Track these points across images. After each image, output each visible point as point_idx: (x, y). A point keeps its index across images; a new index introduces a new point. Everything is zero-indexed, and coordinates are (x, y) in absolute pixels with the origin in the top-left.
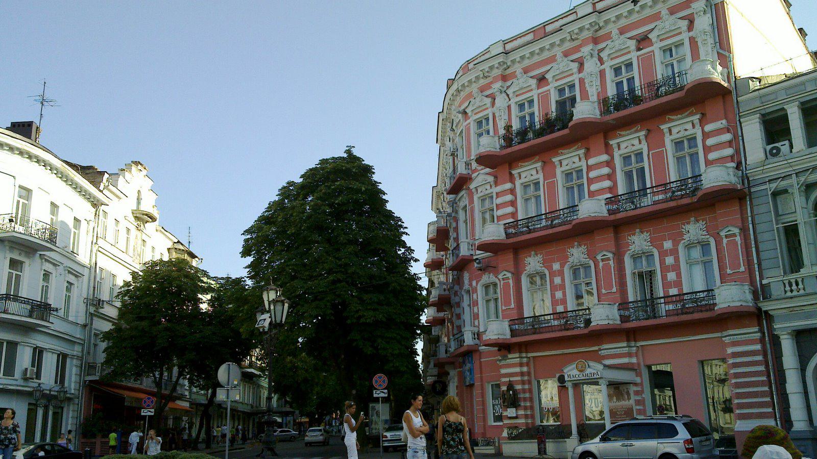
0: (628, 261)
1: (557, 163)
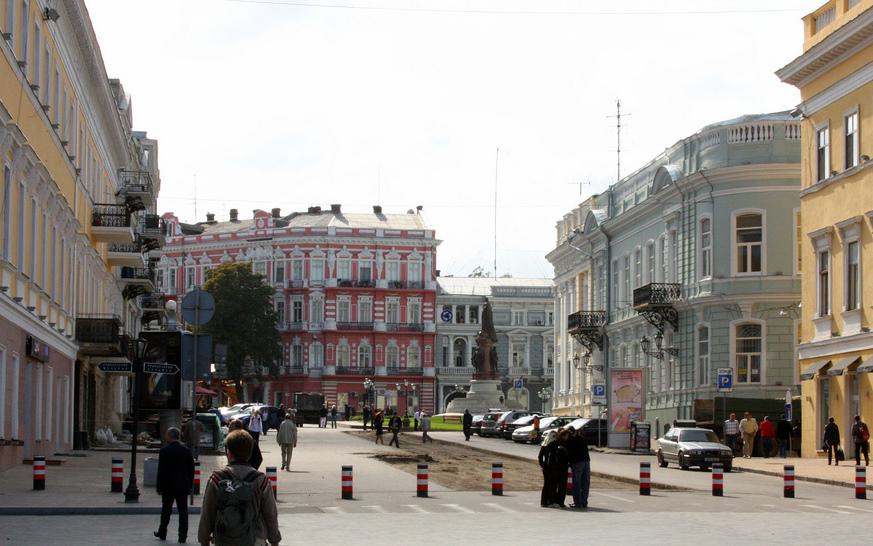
0: (386, 350)
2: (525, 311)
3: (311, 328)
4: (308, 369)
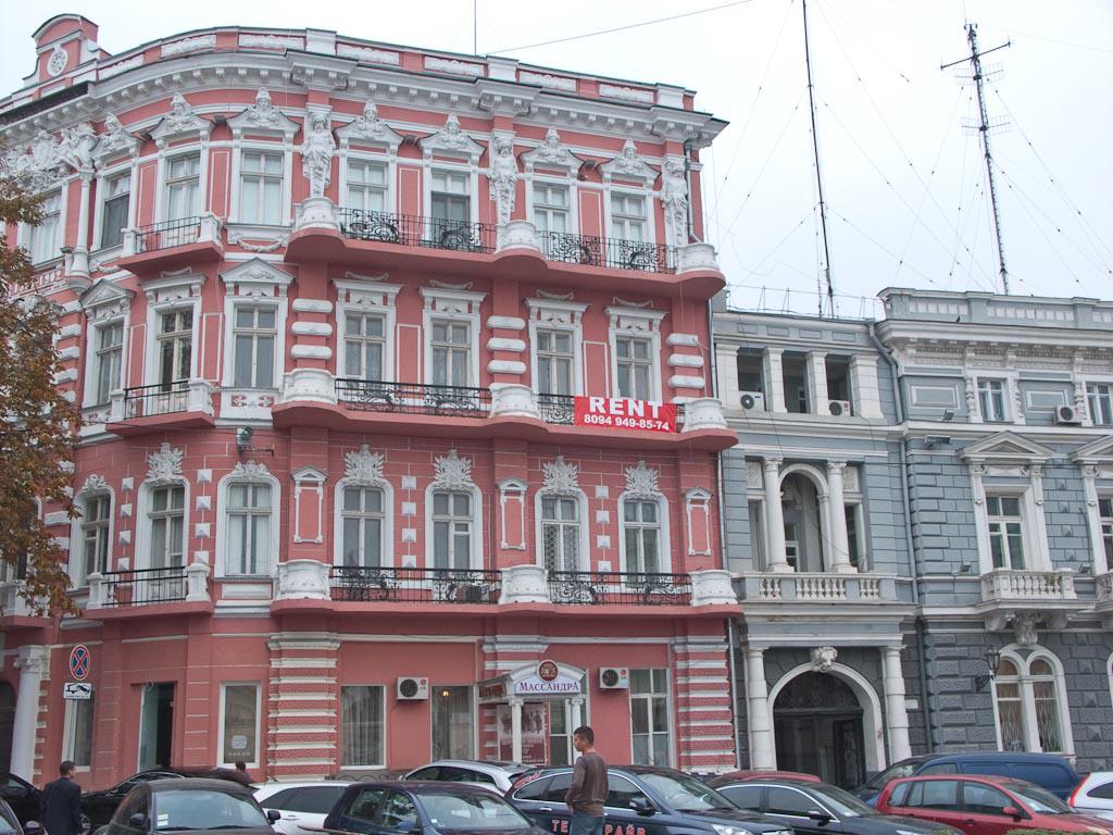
1: (428, 300)
2: (1011, 375)
3: (228, 411)
4: (213, 585)
